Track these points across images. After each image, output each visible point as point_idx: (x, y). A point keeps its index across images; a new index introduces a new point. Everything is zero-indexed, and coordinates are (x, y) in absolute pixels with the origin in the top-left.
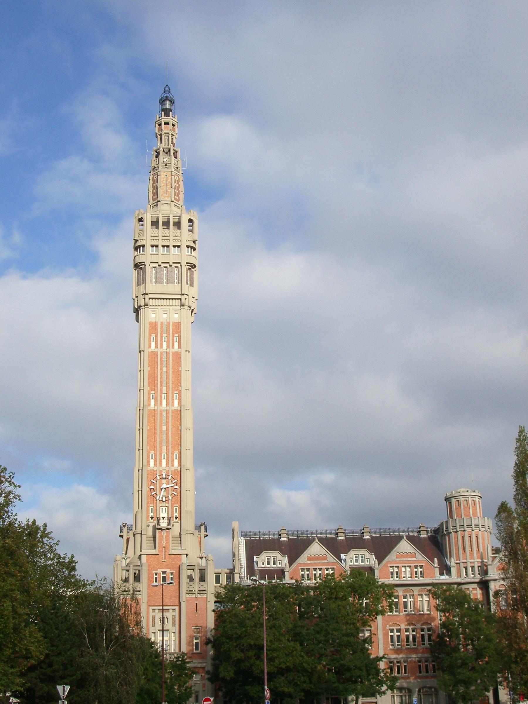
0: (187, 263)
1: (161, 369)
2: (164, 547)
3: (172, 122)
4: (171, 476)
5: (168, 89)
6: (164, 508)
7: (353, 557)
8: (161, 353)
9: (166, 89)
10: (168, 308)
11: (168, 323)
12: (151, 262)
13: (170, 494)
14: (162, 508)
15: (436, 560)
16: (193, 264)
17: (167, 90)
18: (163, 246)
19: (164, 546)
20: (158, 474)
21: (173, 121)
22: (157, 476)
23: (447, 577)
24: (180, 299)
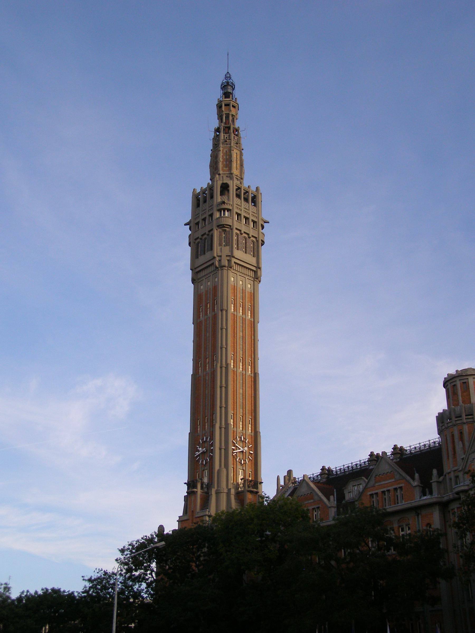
0: (218, 226)
1: (205, 336)
2: (193, 511)
3: (224, 103)
4: (209, 437)
5: (229, 76)
6: (206, 471)
7: (350, 490)
8: (206, 320)
9: (227, 76)
10: (210, 275)
11: (210, 289)
12: (196, 239)
13: (209, 455)
14: (205, 472)
15: (417, 475)
16: (224, 225)
17: (228, 76)
18: (204, 220)
19: (192, 510)
20: (201, 438)
21: (225, 102)
22: (200, 440)
23: (429, 497)
24: (213, 264)
